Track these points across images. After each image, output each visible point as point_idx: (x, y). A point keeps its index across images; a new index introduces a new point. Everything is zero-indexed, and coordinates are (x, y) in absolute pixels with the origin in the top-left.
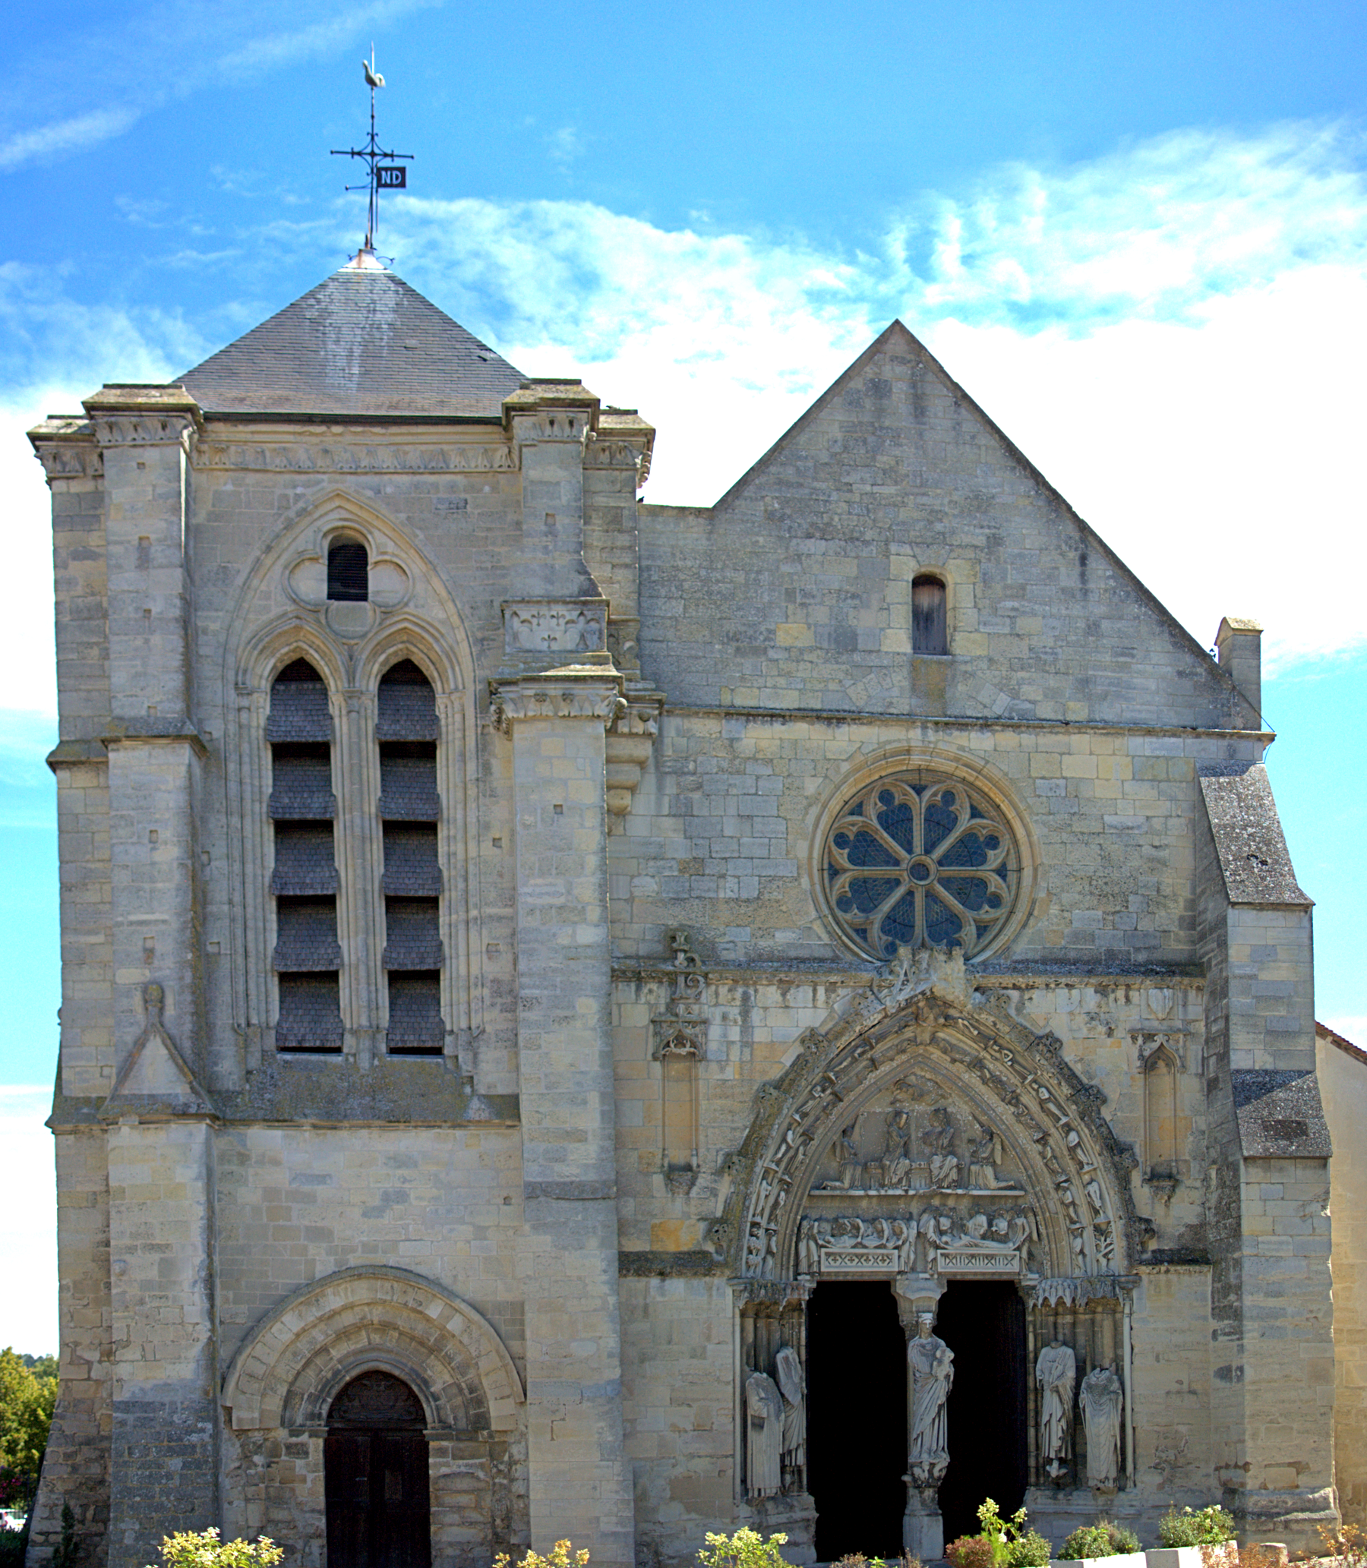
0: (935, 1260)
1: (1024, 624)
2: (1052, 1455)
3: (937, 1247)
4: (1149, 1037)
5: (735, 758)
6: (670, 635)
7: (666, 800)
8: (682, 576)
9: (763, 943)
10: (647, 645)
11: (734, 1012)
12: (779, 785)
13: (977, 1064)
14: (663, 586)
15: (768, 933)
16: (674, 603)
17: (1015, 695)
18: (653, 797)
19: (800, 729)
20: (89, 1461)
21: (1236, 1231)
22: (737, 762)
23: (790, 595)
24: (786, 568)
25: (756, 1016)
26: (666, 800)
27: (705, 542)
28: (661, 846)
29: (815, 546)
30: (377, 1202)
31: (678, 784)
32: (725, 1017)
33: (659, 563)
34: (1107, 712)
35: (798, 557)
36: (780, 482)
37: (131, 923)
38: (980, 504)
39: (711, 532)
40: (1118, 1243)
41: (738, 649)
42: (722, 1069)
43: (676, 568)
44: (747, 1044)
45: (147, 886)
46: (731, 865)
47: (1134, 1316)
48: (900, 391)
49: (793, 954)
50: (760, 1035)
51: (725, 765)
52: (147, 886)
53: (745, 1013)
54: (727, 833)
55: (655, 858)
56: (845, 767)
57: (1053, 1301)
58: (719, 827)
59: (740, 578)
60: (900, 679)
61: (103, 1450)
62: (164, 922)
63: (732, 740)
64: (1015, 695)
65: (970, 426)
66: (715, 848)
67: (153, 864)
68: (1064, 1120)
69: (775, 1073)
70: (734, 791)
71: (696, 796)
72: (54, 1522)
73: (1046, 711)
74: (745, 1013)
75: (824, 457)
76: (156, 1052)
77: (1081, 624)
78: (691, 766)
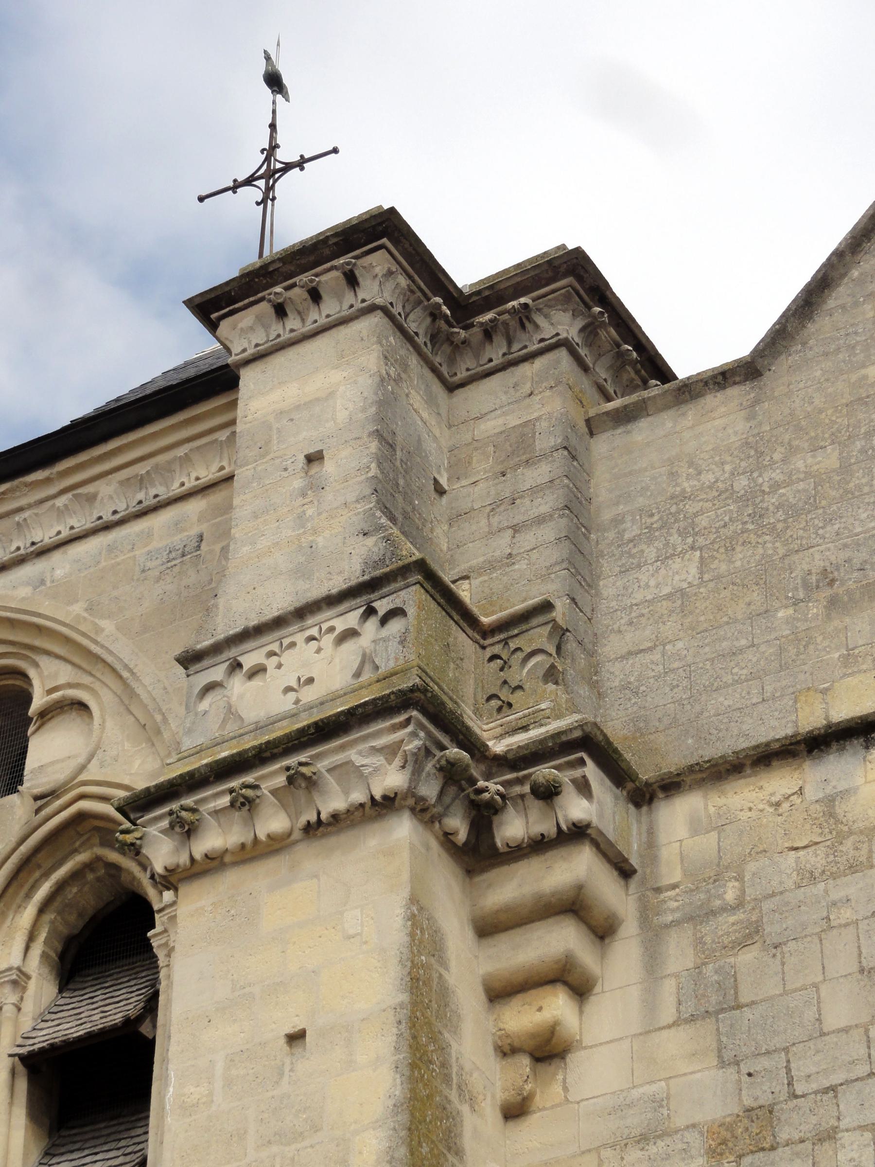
5: (841, 837)
6: (670, 628)
7: (669, 987)
8: (691, 508)
10: (616, 668)
14: (650, 540)
16: (676, 564)
18: (635, 993)
22: (849, 843)
26: (669, 987)
27: (741, 426)
28: (658, 1103)
31: (699, 942)
33: (641, 501)
39: (757, 401)
41: (833, 603)
43: (683, 497)
46: (848, 1100)
51: (815, 859)
54: (831, 1022)
55: (643, 1139)
58: (810, 1014)
59: (829, 459)
63: (830, 801)
66: (800, 1069)
70: (846, 914)
71: (747, 958)
78: (730, 895)
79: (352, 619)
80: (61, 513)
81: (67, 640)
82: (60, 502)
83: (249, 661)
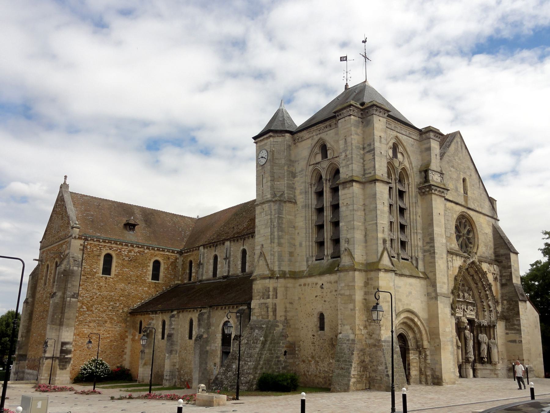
0: (466, 315)
1: (475, 192)
2: (485, 357)
3: (466, 312)
4: (495, 274)
9: (451, 246)
11: (451, 260)
12: (450, 214)
13: (472, 276)
15: (451, 244)
17: (474, 205)
19: (453, 204)
20: (362, 355)
21: (518, 314)
23: (450, 177)
24: (450, 173)
25: (453, 261)
29: (452, 169)
30: (408, 294)
32: (450, 261)
34: (483, 212)
35: (451, 171)
36: (448, 156)
37: (380, 223)
38: (469, 168)
40: (493, 314)
42: (450, 271)
44: (453, 267)
45: (383, 215)
47: (497, 329)
48: (459, 143)
49: (454, 249)
50: (454, 265)
52: (383, 215)
53: (452, 260)
56: (458, 213)
57: (485, 325)
60: (463, 198)
61: (364, 353)
62: (386, 224)
64: (474, 205)
65: (467, 153)
67: (384, 210)
68: (487, 289)
69: (456, 274)
72: (355, 372)
73: (477, 209)
74: (452, 260)
75: (453, 153)
76: (385, 254)
77: (480, 194)
79: (439, 175)
80: (405, 131)
81: (404, 147)
82: (405, 130)
83: (433, 173)
